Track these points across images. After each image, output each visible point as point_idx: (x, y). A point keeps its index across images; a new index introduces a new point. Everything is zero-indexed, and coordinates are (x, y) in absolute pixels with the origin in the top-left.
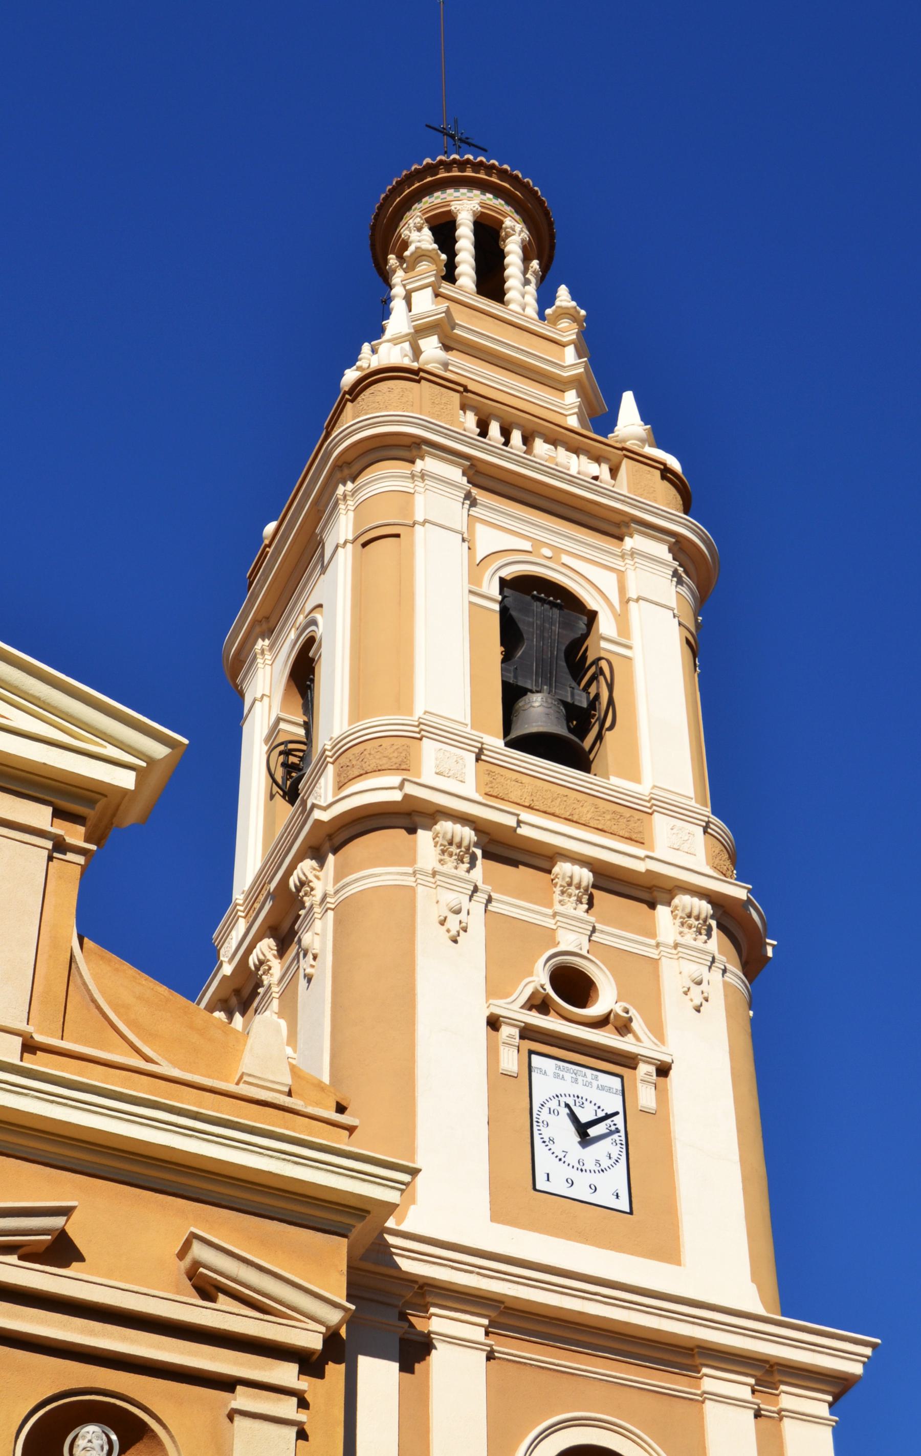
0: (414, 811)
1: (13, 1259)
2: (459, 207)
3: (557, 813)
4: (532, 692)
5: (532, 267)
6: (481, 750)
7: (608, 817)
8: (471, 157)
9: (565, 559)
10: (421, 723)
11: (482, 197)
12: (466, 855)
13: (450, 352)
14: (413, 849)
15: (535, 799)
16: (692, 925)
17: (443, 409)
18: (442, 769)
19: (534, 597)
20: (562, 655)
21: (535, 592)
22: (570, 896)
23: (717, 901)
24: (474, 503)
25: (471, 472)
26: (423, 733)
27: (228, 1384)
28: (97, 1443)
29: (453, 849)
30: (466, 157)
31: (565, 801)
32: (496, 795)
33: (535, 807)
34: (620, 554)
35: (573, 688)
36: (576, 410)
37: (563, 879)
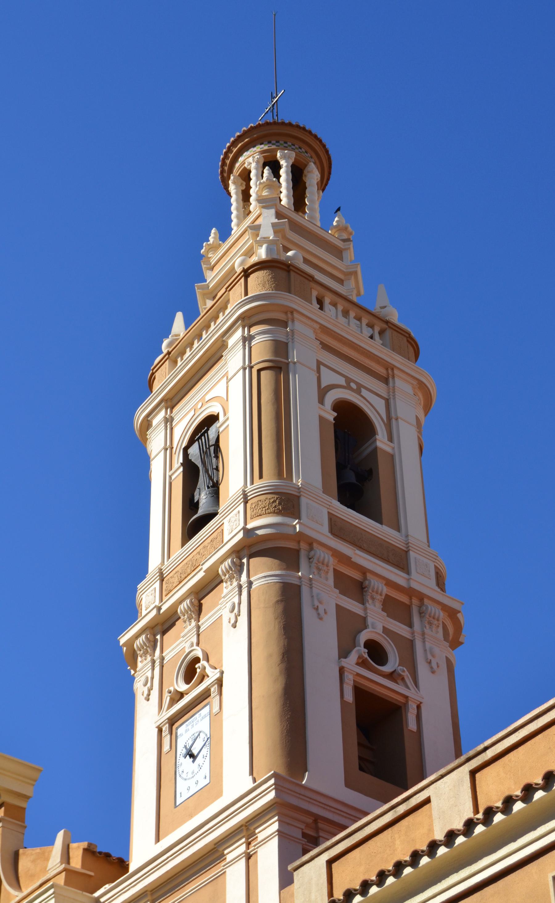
9: (207, 398)
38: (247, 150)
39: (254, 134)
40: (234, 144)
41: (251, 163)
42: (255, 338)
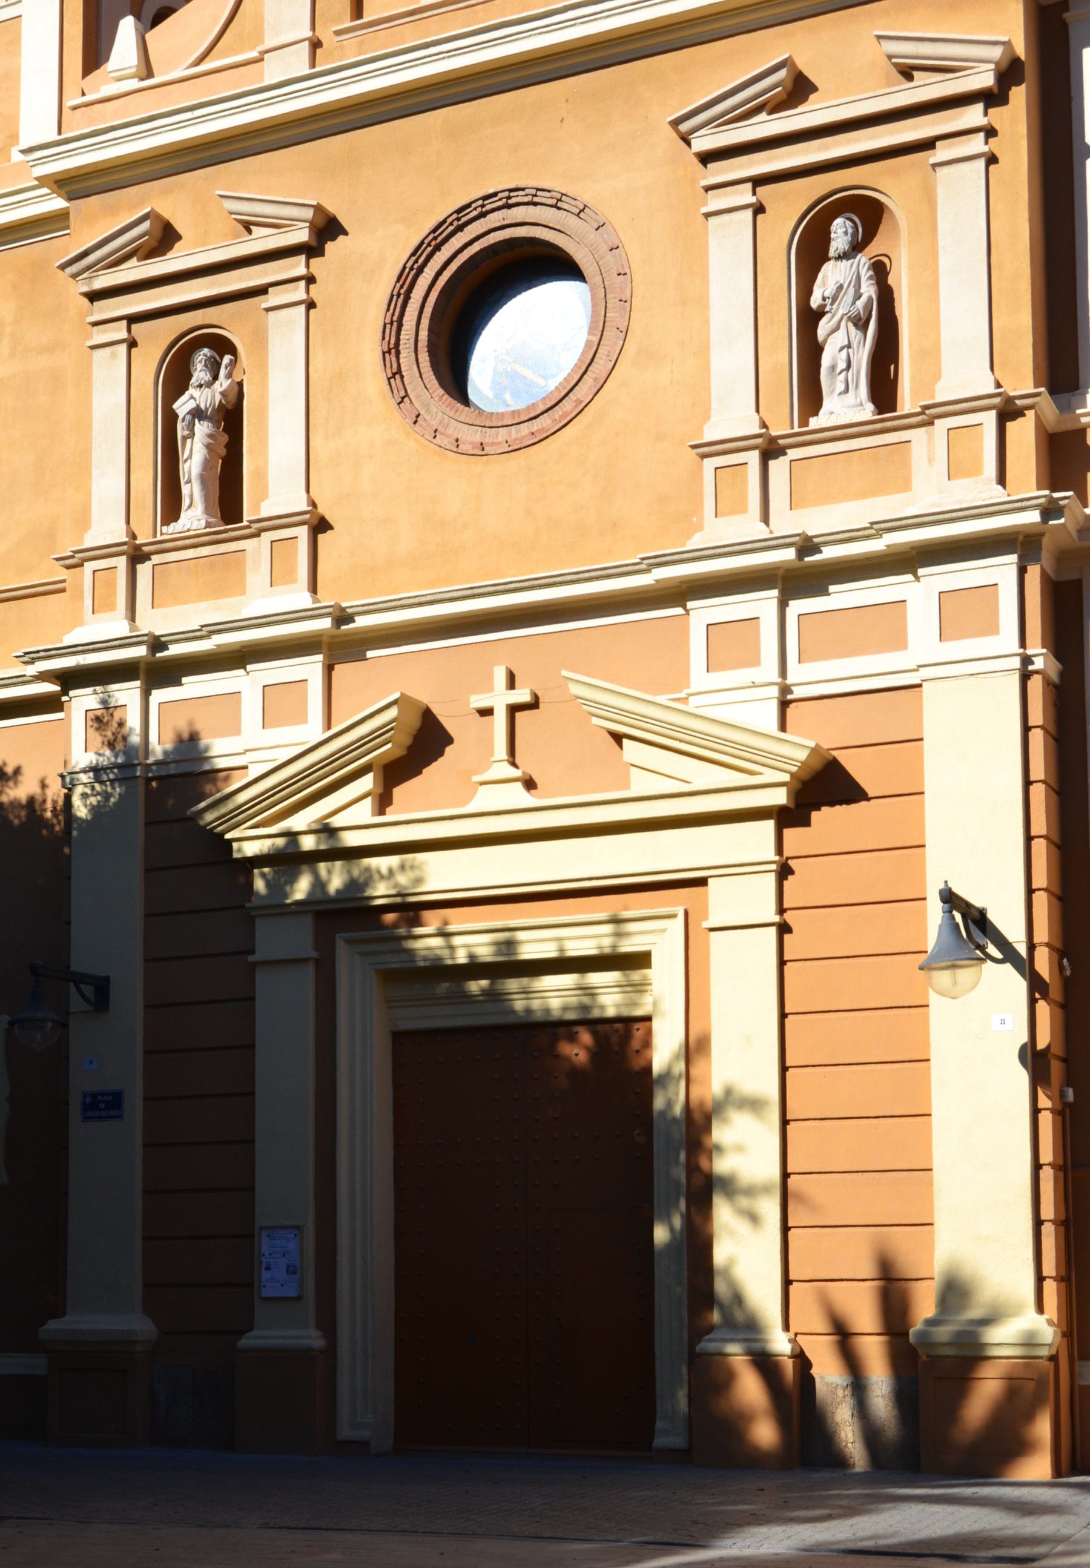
1: (763, 116)
27: (928, 144)
28: (841, 231)
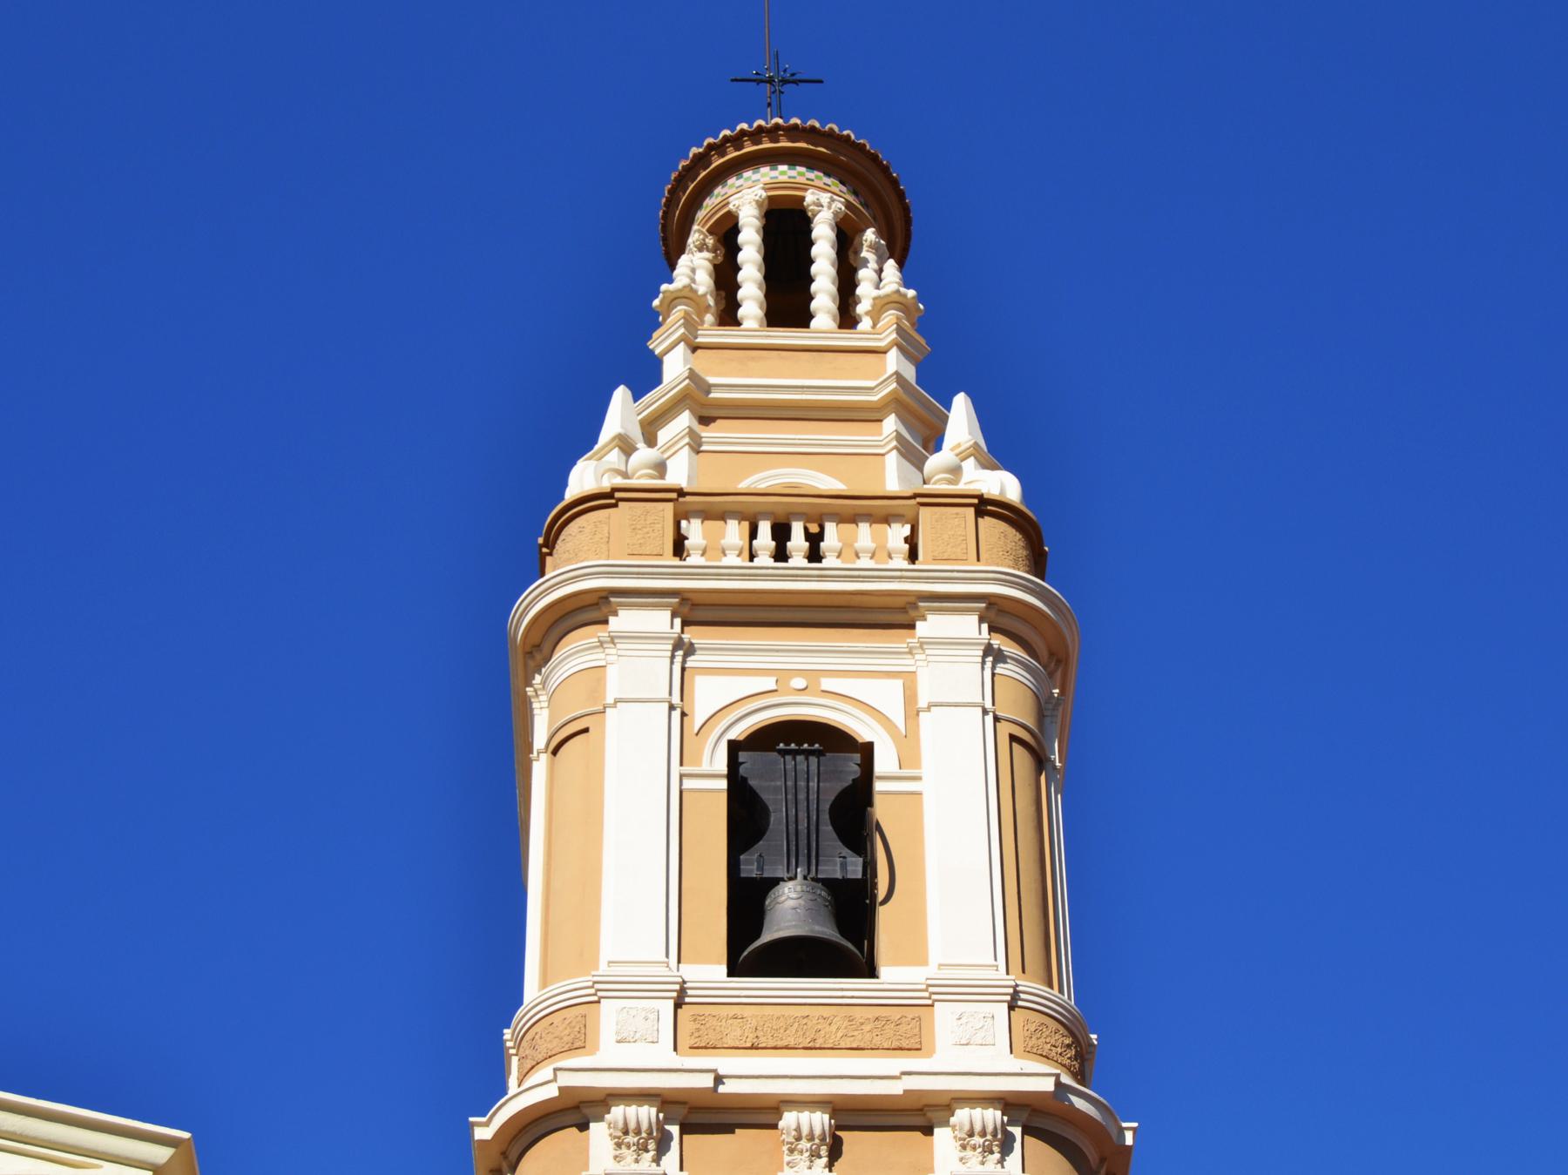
0: (581, 1102)
2: (737, 203)
3: (792, 1044)
4: (782, 880)
5: (866, 241)
6: (682, 992)
7: (867, 1028)
8: (744, 126)
9: (828, 684)
10: (595, 982)
11: (774, 174)
12: (650, 1141)
13: (712, 425)
14: (585, 1150)
15: (760, 1034)
16: (975, 1145)
17: (648, 533)
18: (625, 1035)
19: (783, 753)
20: (825, 817)
21: (782, 745)
22: (801, 1152)
23: (1012, 1105)
24: (690, 650)
25: (686, 609)
26: (600, 994)
29: (631, 1139)
30: (738, 128)
31: (806, 1024)
32: (704, 1045)
33: (760, 1046)
34: (907, 650)
35: (844, 857)
36: (894, 443)
37: (788, 1134)
38: (811, 167)
39: (845, 156)
40: (793, 132)
41: (822, 206)
42: (1008, 663)
